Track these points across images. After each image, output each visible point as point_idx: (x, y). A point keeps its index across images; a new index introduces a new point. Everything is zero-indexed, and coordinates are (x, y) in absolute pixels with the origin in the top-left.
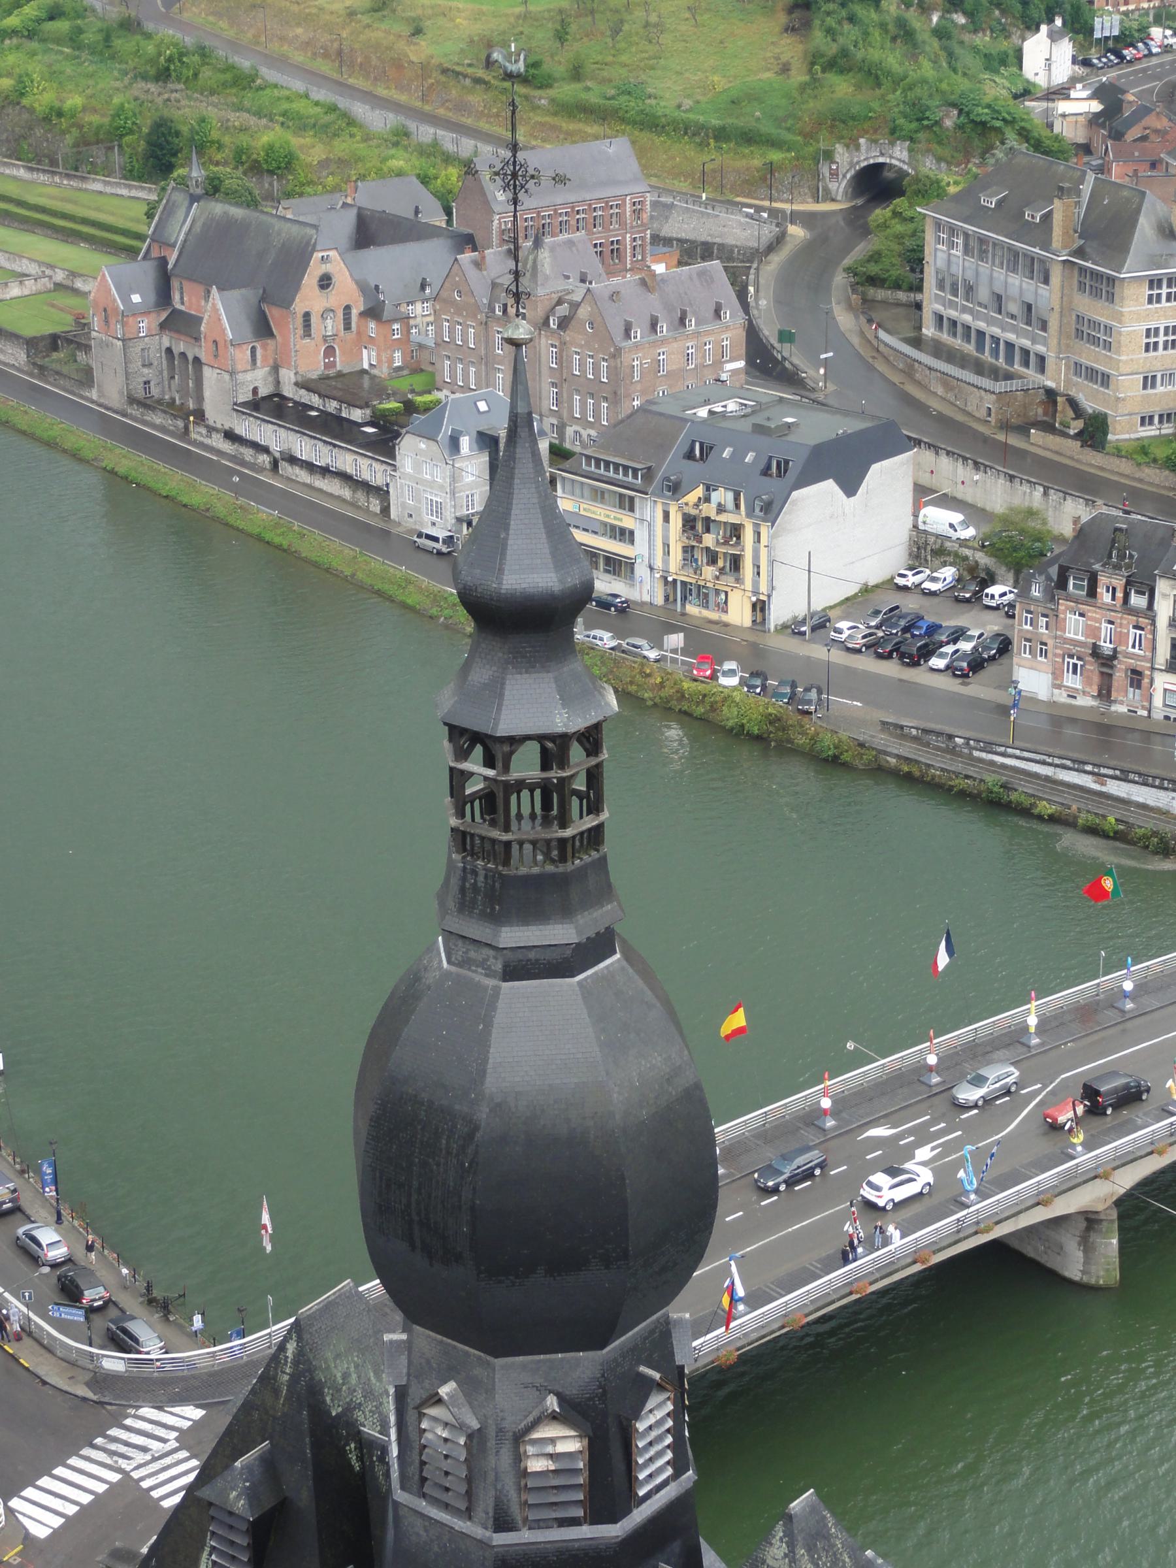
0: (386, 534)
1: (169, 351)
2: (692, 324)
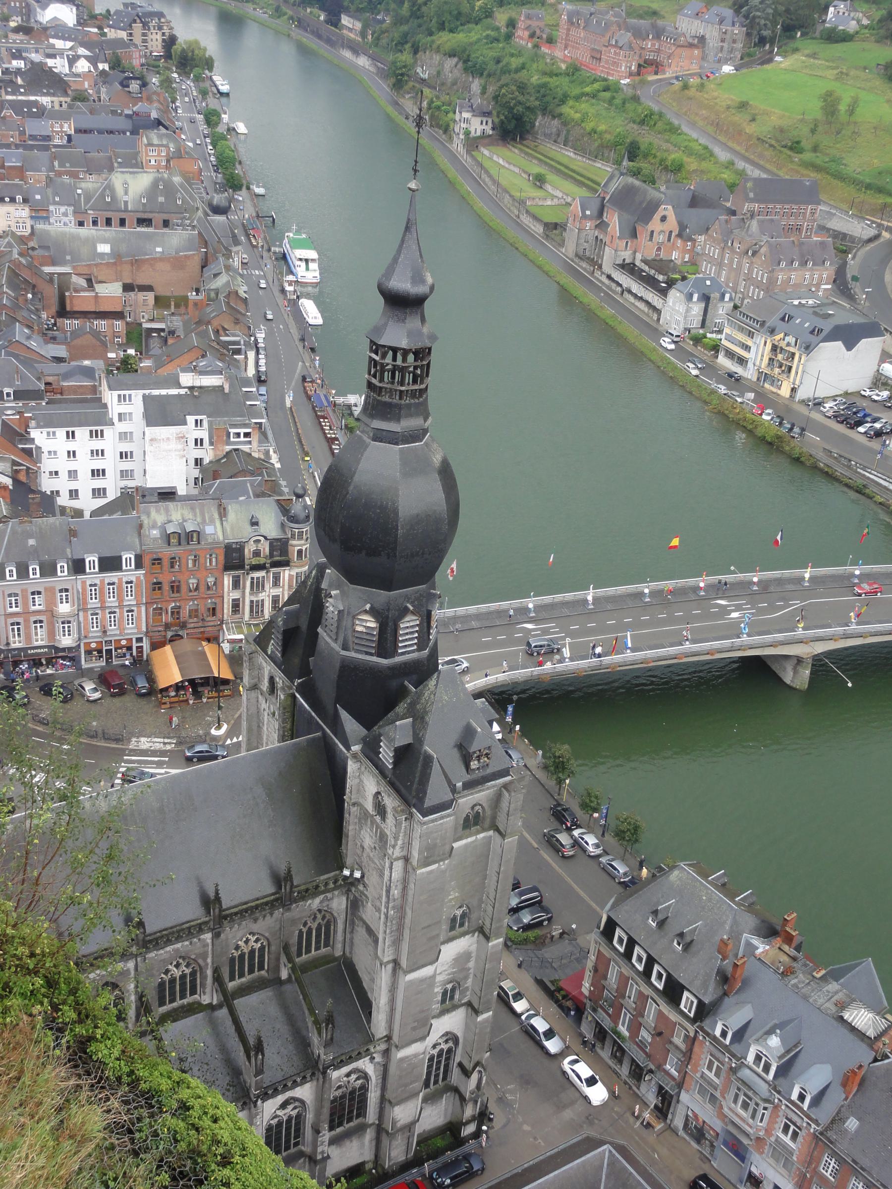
0: (656, 330)
1: (597, 237)
2: (810, 264)
